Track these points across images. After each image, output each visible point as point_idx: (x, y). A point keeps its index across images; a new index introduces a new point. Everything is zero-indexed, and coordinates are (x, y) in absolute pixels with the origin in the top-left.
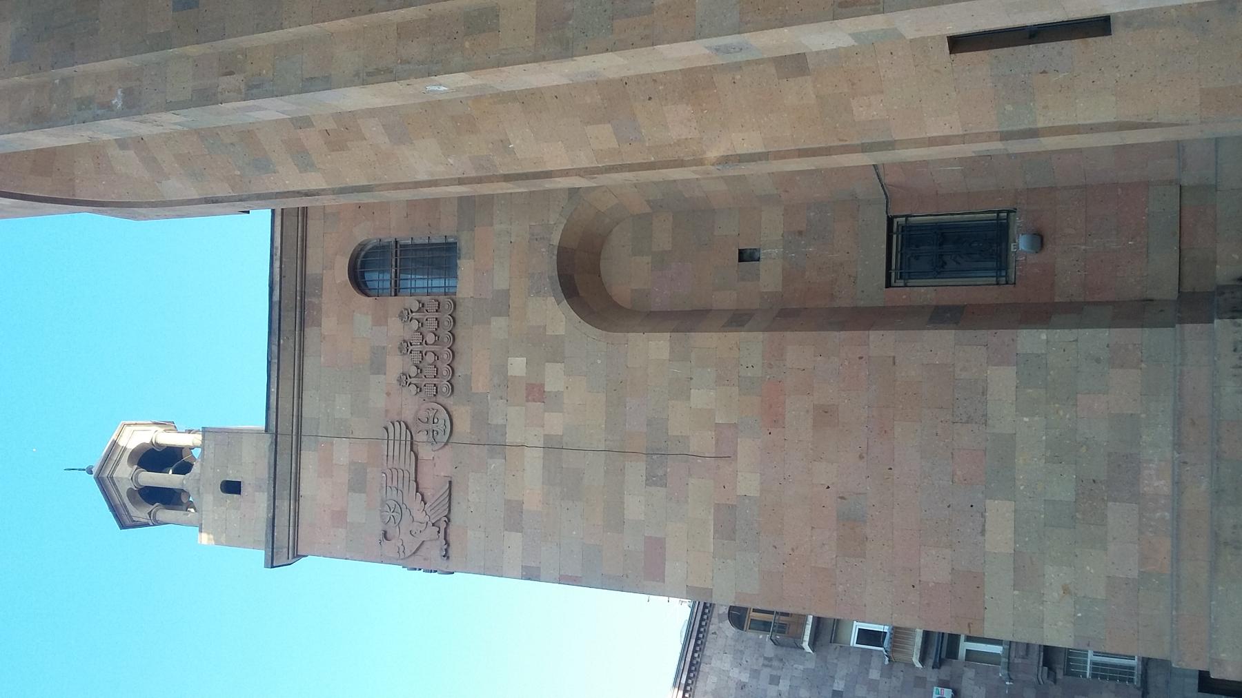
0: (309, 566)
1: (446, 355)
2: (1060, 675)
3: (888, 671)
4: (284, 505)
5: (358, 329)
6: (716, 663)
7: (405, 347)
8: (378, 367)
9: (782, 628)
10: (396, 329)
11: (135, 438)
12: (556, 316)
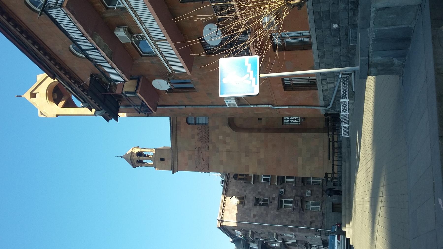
0: (179, 173)
1: (207, 136)
2: (306, 184)
3: (270, 187)
4: (175, 162)
5: (186, 131)
6: (231, 188)
7: (199, 134)
8: (193, 137)
9: (246, 179)
10: (197, 131)
11: (137, 150)
12: (228, 130)
